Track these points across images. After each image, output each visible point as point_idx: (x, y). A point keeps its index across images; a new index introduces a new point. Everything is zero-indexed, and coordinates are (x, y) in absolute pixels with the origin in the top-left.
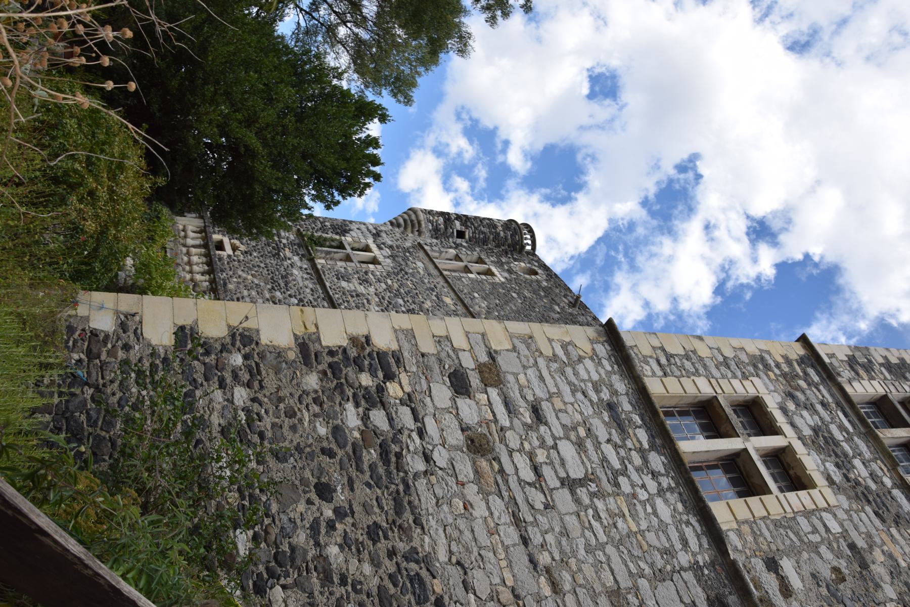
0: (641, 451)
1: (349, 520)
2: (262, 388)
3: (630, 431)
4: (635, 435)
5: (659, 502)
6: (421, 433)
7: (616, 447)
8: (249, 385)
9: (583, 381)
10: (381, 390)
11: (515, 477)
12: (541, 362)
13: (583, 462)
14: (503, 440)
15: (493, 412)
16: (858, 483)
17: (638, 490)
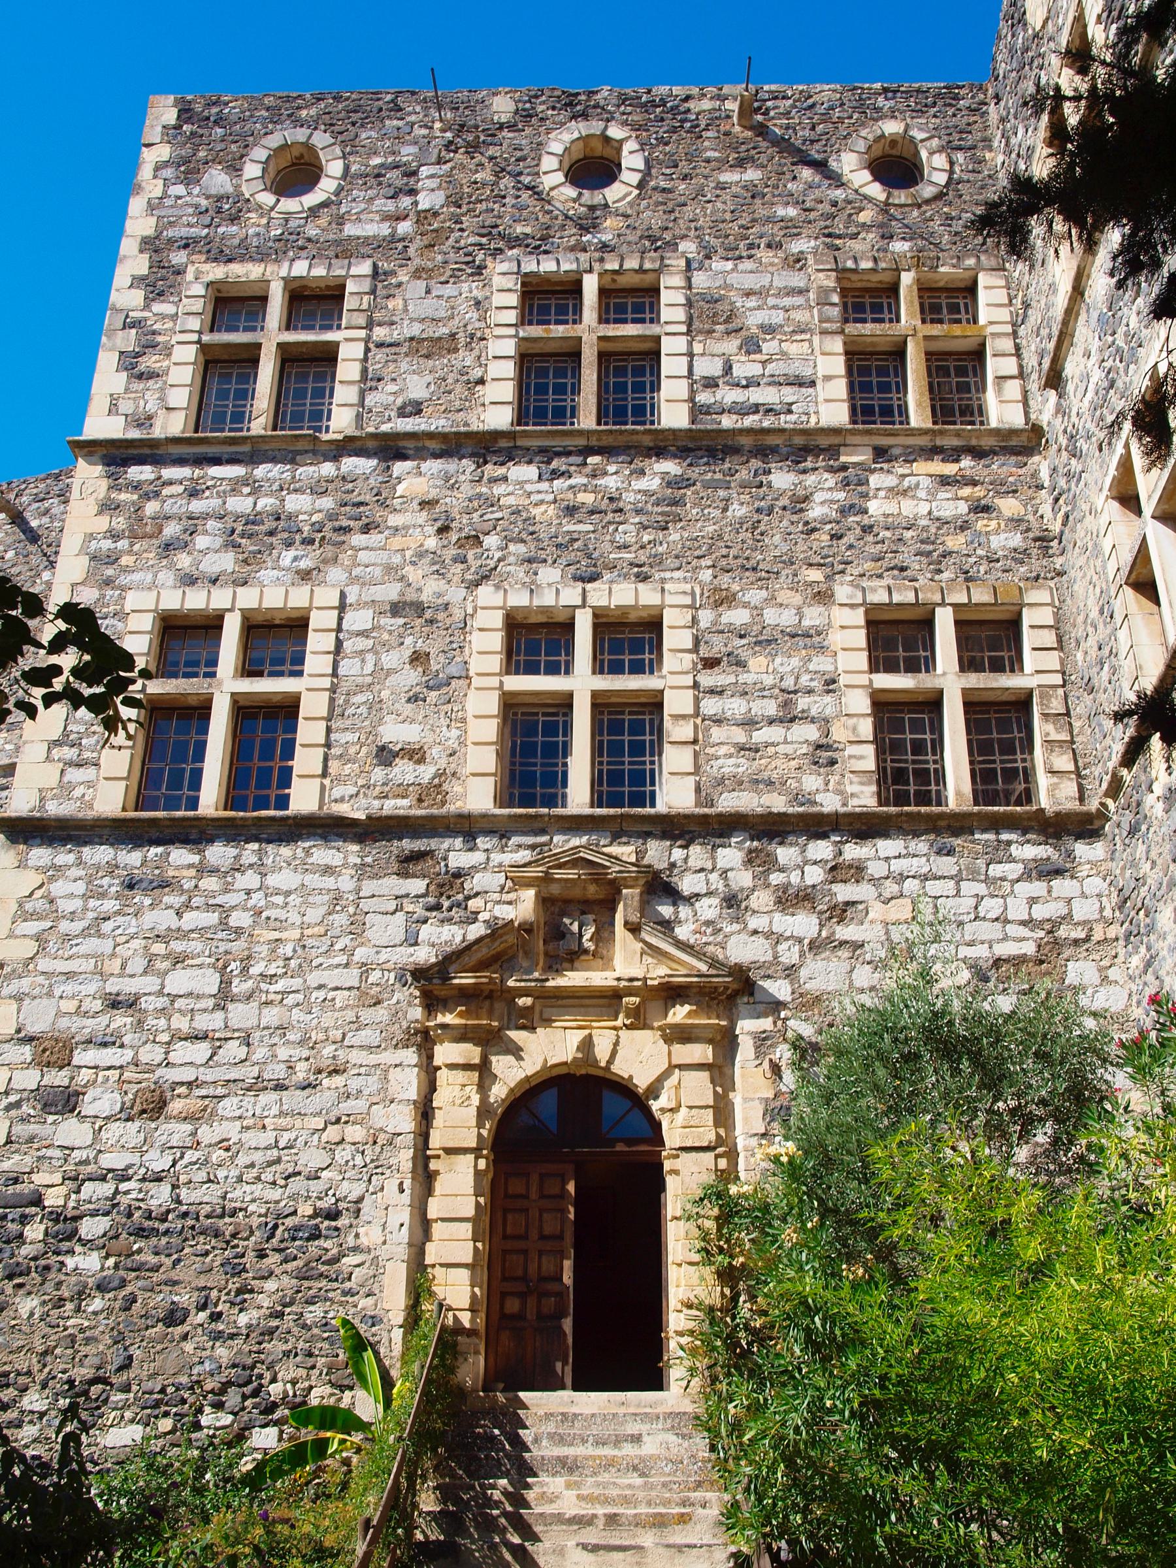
0: (203, 870)
1: (214, 1294)
2: (29, 1373)
3: (171, 873)
4: (177, 868)
5: (272, 880)
6: (123, 1176)
7: (187, 906)
8: (24, 1389)
9: (85, 909)
10: (57, 1217)
11: (202, 1069)
12: (44, 964)
13: (200, 966)
14: (150, 1068)
15: (109, 1068)
16: (319, 527)
17: (251, 903)
